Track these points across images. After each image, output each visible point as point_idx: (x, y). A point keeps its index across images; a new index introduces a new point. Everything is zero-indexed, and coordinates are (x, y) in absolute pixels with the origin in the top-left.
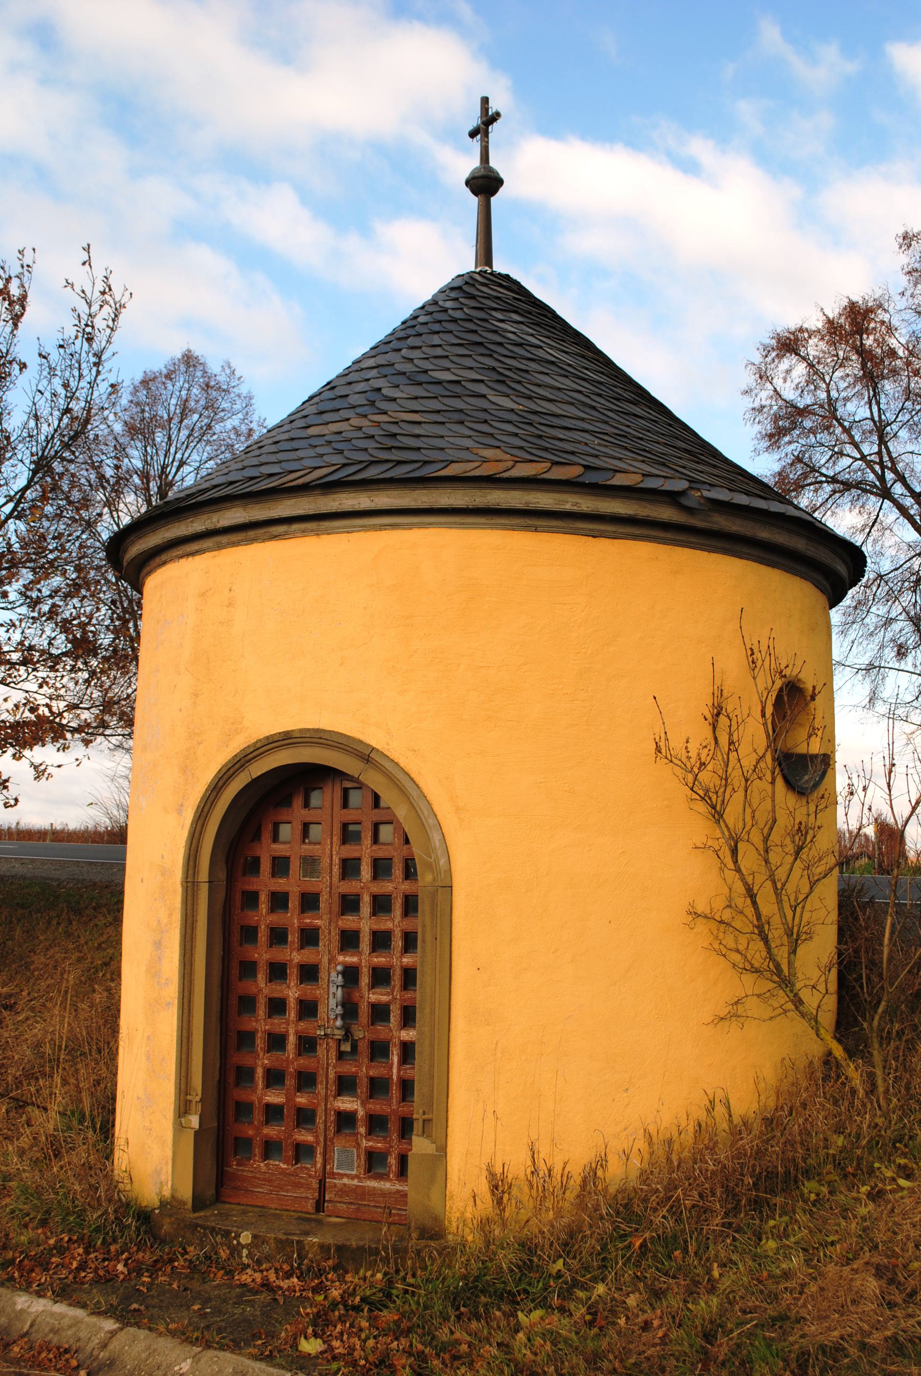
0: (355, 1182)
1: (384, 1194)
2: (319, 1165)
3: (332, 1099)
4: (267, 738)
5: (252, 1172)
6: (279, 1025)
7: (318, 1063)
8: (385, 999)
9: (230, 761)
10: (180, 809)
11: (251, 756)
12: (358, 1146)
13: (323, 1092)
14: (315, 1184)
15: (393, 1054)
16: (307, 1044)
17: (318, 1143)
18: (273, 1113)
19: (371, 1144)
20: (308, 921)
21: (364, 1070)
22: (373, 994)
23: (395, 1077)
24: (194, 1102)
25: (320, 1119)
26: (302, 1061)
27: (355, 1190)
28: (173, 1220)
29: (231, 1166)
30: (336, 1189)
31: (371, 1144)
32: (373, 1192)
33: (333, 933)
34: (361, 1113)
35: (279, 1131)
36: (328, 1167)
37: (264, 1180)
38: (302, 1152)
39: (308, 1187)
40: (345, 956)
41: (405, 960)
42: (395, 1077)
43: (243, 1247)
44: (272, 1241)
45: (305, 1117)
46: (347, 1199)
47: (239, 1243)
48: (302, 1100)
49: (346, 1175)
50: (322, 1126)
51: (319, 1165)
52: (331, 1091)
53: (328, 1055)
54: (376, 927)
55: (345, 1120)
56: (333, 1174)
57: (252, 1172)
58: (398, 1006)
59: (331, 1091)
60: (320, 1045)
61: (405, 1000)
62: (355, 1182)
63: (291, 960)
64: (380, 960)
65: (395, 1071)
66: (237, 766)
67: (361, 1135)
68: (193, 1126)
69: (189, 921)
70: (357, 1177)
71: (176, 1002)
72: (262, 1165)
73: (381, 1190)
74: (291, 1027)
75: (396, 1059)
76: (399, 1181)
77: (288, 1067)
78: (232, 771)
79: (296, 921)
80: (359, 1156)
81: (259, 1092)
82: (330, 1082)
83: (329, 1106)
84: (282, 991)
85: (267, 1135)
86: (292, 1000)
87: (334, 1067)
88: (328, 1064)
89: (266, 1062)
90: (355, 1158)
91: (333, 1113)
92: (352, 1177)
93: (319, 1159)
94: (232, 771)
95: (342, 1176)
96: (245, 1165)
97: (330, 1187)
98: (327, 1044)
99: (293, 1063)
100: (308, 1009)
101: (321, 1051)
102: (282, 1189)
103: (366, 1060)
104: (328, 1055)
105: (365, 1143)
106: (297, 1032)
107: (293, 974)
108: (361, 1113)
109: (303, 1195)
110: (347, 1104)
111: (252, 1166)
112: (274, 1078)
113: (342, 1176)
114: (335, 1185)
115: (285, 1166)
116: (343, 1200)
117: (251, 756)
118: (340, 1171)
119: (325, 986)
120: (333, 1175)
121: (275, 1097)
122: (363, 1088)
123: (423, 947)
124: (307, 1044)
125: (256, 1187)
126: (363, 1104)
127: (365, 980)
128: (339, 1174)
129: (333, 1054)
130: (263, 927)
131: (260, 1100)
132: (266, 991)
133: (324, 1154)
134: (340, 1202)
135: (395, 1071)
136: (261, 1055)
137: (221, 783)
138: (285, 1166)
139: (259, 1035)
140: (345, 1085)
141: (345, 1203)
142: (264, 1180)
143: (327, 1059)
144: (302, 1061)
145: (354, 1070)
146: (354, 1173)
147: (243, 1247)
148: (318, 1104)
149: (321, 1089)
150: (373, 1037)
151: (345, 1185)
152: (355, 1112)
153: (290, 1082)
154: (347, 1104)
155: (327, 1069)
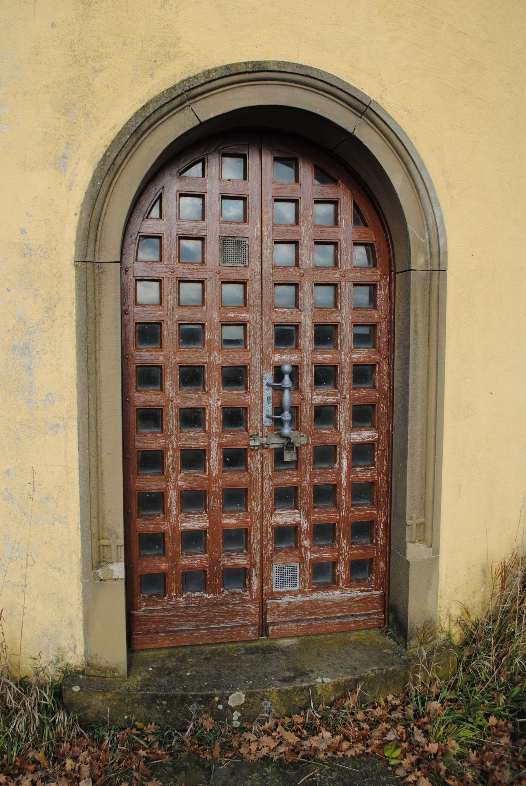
0: (300, 598)
1: (336, 604)
2: (255, 588)
3: (268, 515)
4: (227, 67)
5: (169, 610)
6: (197, 439)
7: (251, 477)
8: (331, 399)
9: (162, 95)
10: (61, 163)
11: (200, 90)
12: (302, 561)
13: (258, 509)
14: (254, 609)
15: (341, 458)
16: (234, 458)
17: (252, 564)
18: (192, 539)
19: (317, 555)
20: (232, 315)
21: (308, 478)
22: (317, 395)
23: (344, 483)
24: (114, 547)
25: (254, 540)
26: (229, 478)
27: (302, 607)
28: (109, 696)
29: (138, 608)
30: (280, 609)
31: (317, 555)
32: (324, 605)
33: (265, 329)
34: (305, 525)
35: (202, 560)
36: (266, 588)
37: (188, 616)
38: (240, 575)
39: (246, 613)
40: (281, 353)
41: (355, 356)
42: (344, 483)
43: (233, 710)
44: (274, 695)
45: (238, 537)
46: (294, 617)
47: (226, 707)
48: (230, 521)
49: (288, 592)
50: (257, 546)
51: (255, 588)
52: (268, 506)
53: (262, 467)
54: (320, 321)
55: (286, 534)
56: (272, 593)
57: (169, 610)
58: (347, 406)
59: (268, 506)
60: (252, 457)
61: (355, 399)
62: (300, 598)
63: (210, 363)
64: (325, 357)
65: (344, 476)
66: (176, 102)
67: (305, 548)
68: (115, 576)
69: (91, 315)
70: (300, 591)
71: (75, 423)
72: (181, 600)
73: (332, 600)
74: (214, 440)
75: (345, 463)
76: (350, 587)
77: (210, 486)
78: (166, 109)
79: (215, 315)
80: (302, 571)
81: (173, 519)
82: (266, 496)
83: (265, 523)
84: (200, 399)
85: (185, 567)
86: (213, 408)
87: (271, 480)
88: (262, 477)
89: (180, 483)
90: (298, 573)
91: (270, 530)
92: (296, 594)
93: (255, 582)
94: (166, 109)
95: (282, 594)
96: (157, 603)
97: (272, 609)
98: (262, 455)
99: (217, 481)
100: (234, 417)
101: (253, 463)
102: (211, 621)
103: (310, 468)
104: (262, 467)
105: (309, 556)
106: (221, 445)
107: (213, 379)
108: (305, 525)
109: (240, 623)
110: (286, 517)
111: (168, 603)
112: (193, 500)
113: (282, 594)
114: (278, 606)
115: (211, 596)
116: (288, 619)
117: (200, 90)
118: (280, 590)
119: (258, 390)
120: (272, 595)
121: (195, 522)
122: (306, 498)
123: (415, 339)
124: (234, 458)
125: (177, 625)
126: (307, 515)
127: (307, 379)
128: (279, 593)
129: (269, 463)
130: (170, 323)
131: (174, 529)
132: (178, 401)
133: (261, 575)
134: (285, 622)
135: (344, 476)
136: (174, 476)
137: (146, 125)
138: (211, 596)
139: (170, 453)
140: (286, 496)
141: (291, 622)
142: (188, 616)
143: (262, 472)
144: (229, 478)
145: (295, 480)
146: (297, 588)
147: (233, 710)
148: (253, 523)
149: (255, 505)
150: (318, 442)
151: (290, 603)
152: (296, 527)
153: (214, 503)
154: (286, 517)
155: (262, 482)
